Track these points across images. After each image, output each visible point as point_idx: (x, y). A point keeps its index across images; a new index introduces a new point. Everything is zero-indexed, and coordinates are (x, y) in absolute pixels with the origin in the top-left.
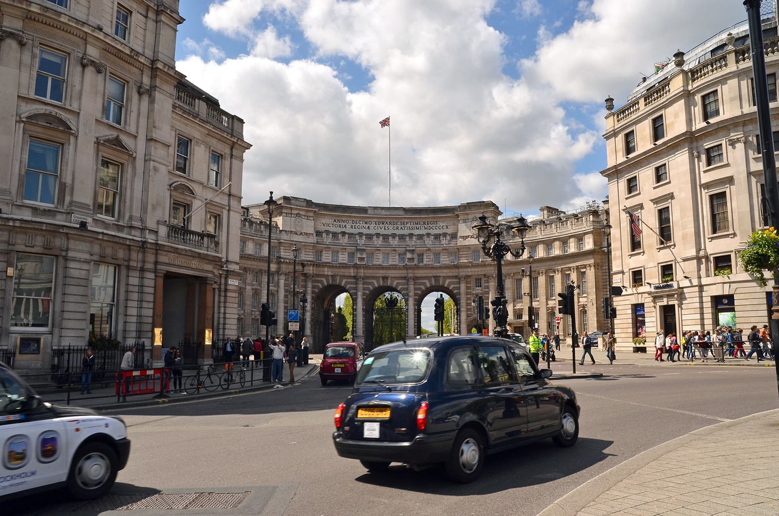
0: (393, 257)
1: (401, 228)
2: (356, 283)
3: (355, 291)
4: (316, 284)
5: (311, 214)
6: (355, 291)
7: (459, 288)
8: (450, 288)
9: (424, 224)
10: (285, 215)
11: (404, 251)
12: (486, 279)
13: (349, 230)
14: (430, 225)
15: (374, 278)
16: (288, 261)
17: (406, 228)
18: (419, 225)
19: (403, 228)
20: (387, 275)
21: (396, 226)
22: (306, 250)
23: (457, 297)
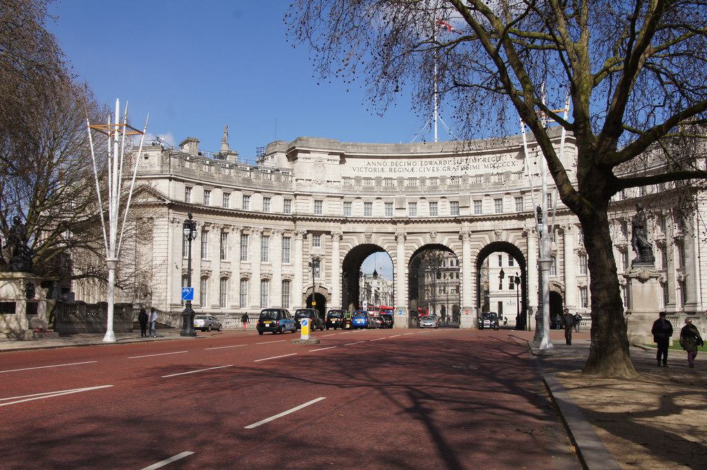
5: (338, 157)
9: (484, 160)
10: (303, 160)
11: (456, 200)
18: (477, 163)
21: (447, 165)
22: (330, 203)
23: (525, 255)
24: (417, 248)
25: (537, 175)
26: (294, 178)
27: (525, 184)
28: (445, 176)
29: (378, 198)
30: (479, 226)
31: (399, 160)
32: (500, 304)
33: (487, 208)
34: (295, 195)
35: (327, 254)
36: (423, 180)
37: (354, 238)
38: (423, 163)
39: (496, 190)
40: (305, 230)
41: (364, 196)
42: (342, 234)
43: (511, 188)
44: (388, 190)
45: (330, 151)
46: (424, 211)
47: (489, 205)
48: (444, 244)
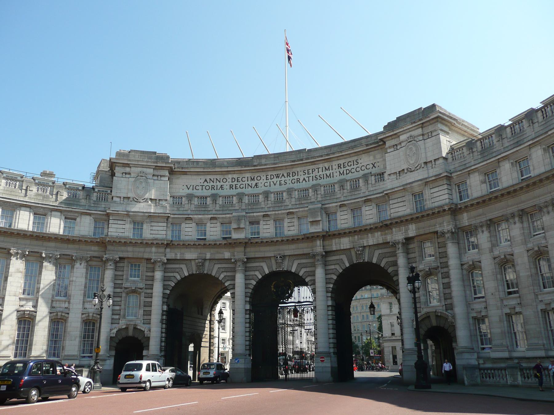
0: (290, 224)
1: (304, 179)
2: (234, 270)
3: (232, 282)
4: (172, 274)
6: (232, 282)
7: (395, 264)
8: (382, 265)
12: (441, 240)
13: (227, 192)
14: (348, 168)
15: (263, 259)
16: (118, 241)
17: (311, 178)
18: (331, 171)
19: (307, 179)
20: (282, 253)
21: (296, 177)
22: (153, 224)
23: (395, 279)
24: (260, 277)
25: (403, 170)
26: (110, 197)
27: (390, 183)
28: (292, 188)
29: (212, 219)
30: (335, 244)
31: (241, 176)
32: (394, 348)
33: (343, 222)
34: (108, 215)
35: (147, 286)
36: (266, 194)
37: (183, 267)
38: (269, 177)
39: (353, 197)
40: (117, 257)
41: (196, 216)
42: (166, 261)
43: (372, 193)
44: (226, 209)
45: (156, 165)
46: (268, 231)
47: (345, 217)
48: (293, 270)
